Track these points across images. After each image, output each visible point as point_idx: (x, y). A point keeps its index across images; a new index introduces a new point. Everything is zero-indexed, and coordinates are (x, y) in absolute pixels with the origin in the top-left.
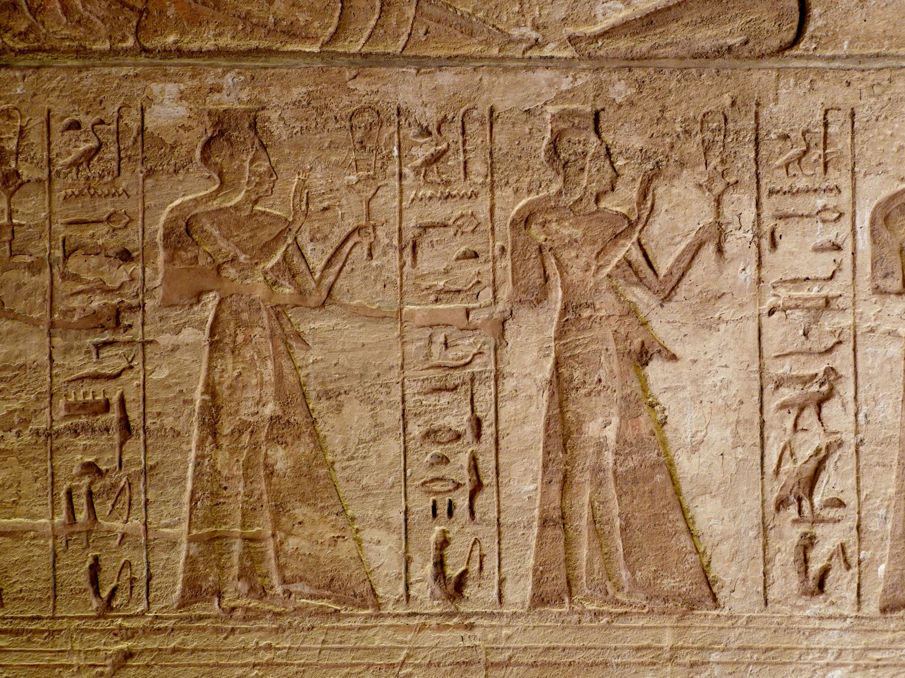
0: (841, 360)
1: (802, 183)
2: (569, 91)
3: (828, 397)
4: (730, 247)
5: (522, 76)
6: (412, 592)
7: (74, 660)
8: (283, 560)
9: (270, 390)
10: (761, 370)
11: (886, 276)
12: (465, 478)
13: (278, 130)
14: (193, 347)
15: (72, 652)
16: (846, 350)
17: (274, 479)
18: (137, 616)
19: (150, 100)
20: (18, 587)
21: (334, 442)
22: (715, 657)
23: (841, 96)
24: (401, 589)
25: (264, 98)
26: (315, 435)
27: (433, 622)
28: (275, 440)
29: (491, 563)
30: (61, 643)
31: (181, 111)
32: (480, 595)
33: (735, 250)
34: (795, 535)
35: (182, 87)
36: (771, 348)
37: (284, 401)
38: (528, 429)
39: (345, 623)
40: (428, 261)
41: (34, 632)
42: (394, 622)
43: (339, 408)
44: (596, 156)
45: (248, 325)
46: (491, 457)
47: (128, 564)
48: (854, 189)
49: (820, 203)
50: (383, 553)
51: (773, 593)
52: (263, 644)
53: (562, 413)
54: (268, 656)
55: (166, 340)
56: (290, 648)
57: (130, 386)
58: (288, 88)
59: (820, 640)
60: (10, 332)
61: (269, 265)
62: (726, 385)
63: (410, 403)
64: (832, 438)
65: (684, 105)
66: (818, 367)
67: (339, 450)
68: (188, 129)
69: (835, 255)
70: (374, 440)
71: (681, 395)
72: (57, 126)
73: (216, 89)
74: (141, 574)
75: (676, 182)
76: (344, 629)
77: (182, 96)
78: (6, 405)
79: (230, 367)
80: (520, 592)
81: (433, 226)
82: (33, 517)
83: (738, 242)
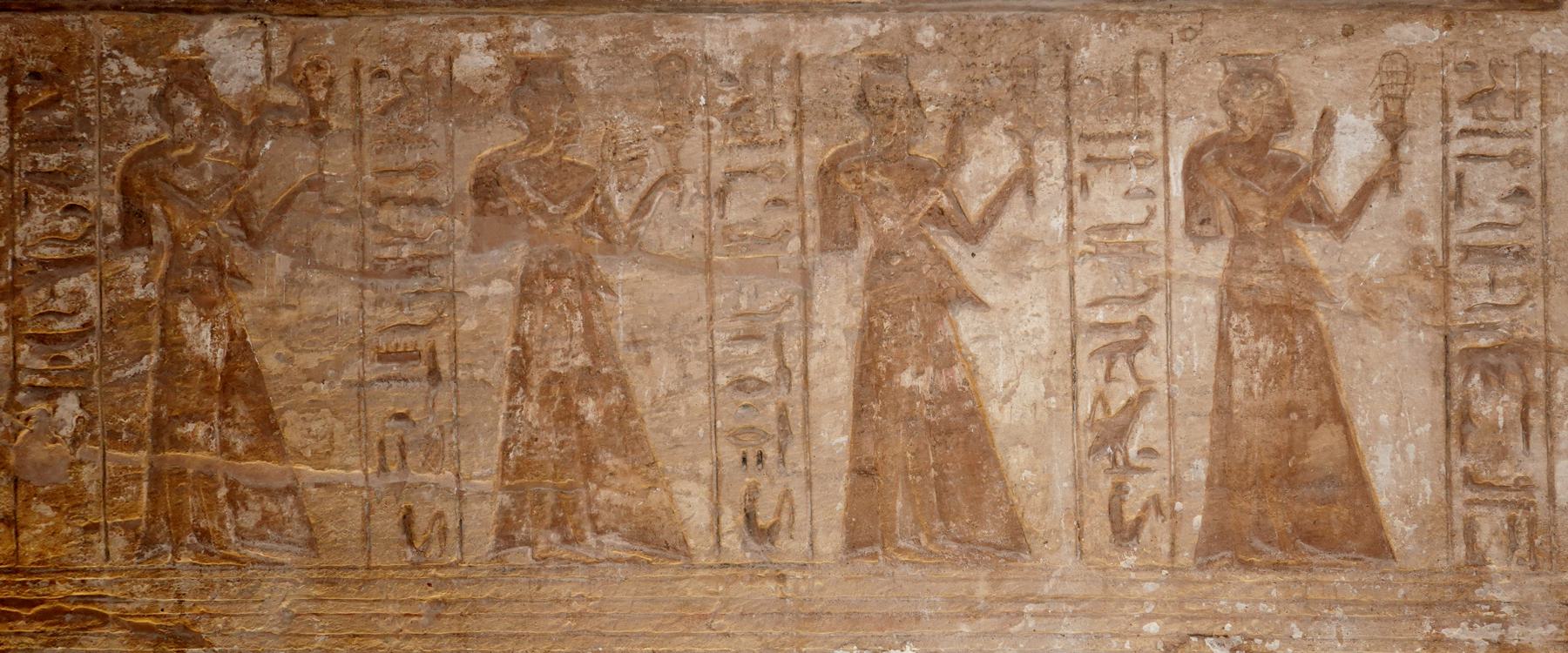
0: (1154, 308)
1: (1114, 128)
2: (878, 38)
3: (1138, 345)
4: (1042, 192)
5: (831, 21)
6: (723, 544)
7: (391, 609)
8: (595, 511)
9: (578, 341)
10: (1073, 317)
11: (1202, 223)
12: (772, 427)
13: (586, 81)
14: (502, 299)
15: (387, 601)
16: (1159, 297)
17: (585, 431)
18: (450, 566)
19: (457, 50)
20: (333, 536)
21: (643, 394)
22: (1029, 608)
23: (1155, 40)
24: (712, 541)
25: (571, 47)
26: (625, 387)
27: (745, 573)
28: (587, 391)
29: (801, 515)
30: (374, 593)
31: (489, 61)
32: (791, 547)
33: (1047, 197)
34: (1106, 485)
35: (490, 36)
36: (1082, 298)
37: (595, 357)
38: (837, 380)
39: (658, 574)
40: (736, 212)
41: (349, 581)
42: (707, 573)
43: (647, 360)
44: (905, 102)
45: (557, 277)
46: (799, 409)
47: (440, 515)
48: (1165, 132)
49: (1132, 149)
50: (693, 506)
51: (1088, 545)
52: (575, 594)
53: (875, 362)
54: (577, 607)
55: (475, 291)
56: (603, 599)
57: (441, 337)
58: (594, 37)
59: (1135, 592)
60: (321, 284)
61: (578, 215)
62: (1037, 334)
63: (719, 350)
64: (1146, 387)
65: (994, 51)
66: (1131, 316)
67: (649, 402)
68: (494, 78)
69: (1148, 202)
70: (682, 391)
71: (991, 345)
72: (365, 76)
73: (525, 38)
74: (452, 525)
75: (986, 129)
76: (656, 580)
77: (490, 46)
78: (317, 356)
79: (540, 318)
80: (830, 542)
81: (742, 173)
82: (347, 468)
83: (1050, 186)
